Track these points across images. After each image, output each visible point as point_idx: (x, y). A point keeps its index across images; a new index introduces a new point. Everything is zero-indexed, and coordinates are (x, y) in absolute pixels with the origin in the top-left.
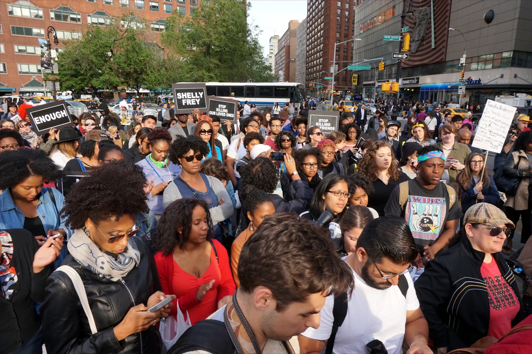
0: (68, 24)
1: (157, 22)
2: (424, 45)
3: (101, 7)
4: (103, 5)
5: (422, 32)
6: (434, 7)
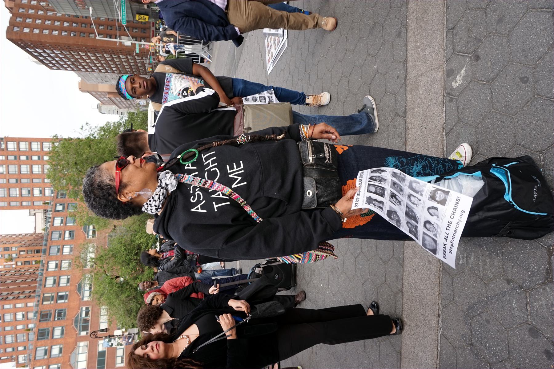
0: (91, 319)
1: (86, 232)
3: (73, 288)
4: (71, 285)
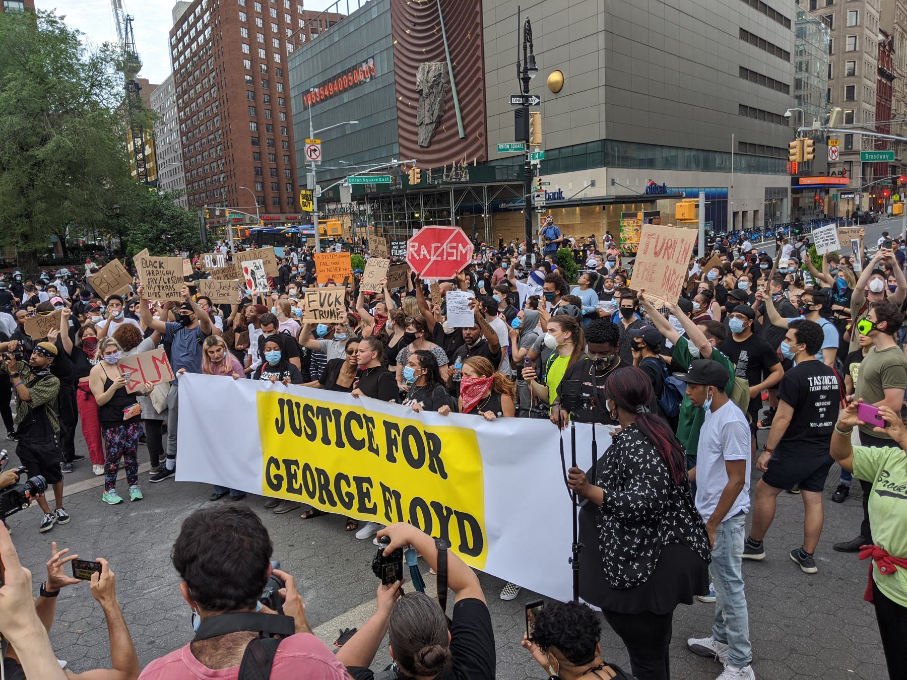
2: (443, 131)
5: (437, 107)
6: (452, 61)
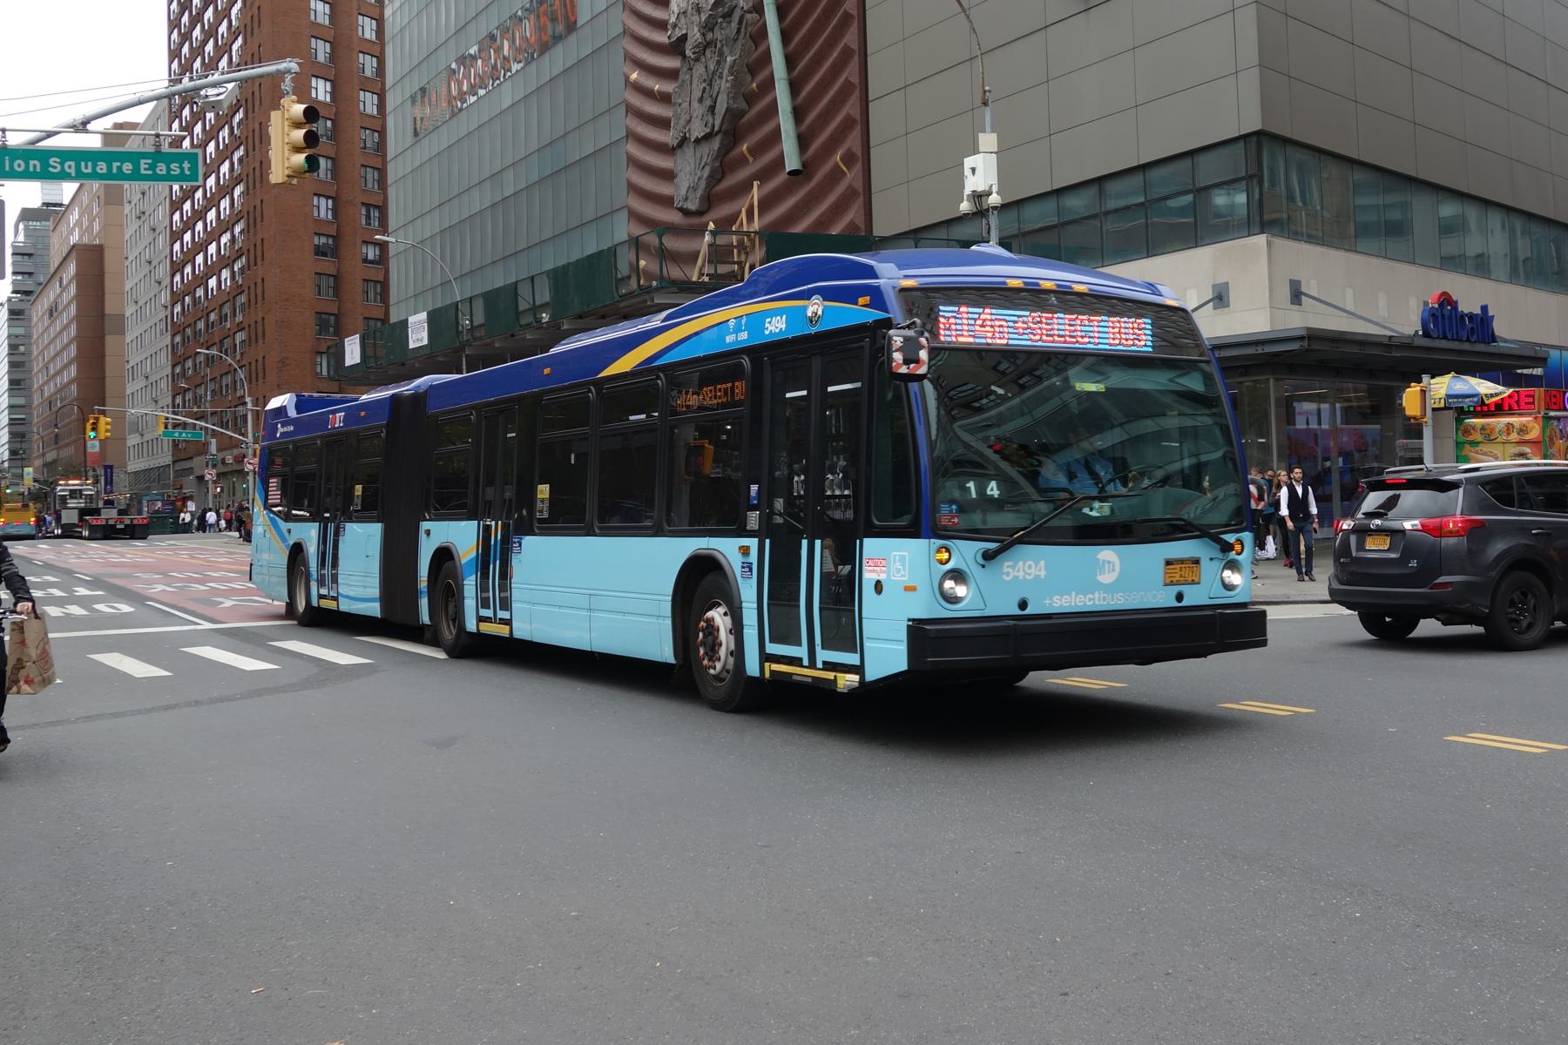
2: (742, 161)
5: (724, 85)
